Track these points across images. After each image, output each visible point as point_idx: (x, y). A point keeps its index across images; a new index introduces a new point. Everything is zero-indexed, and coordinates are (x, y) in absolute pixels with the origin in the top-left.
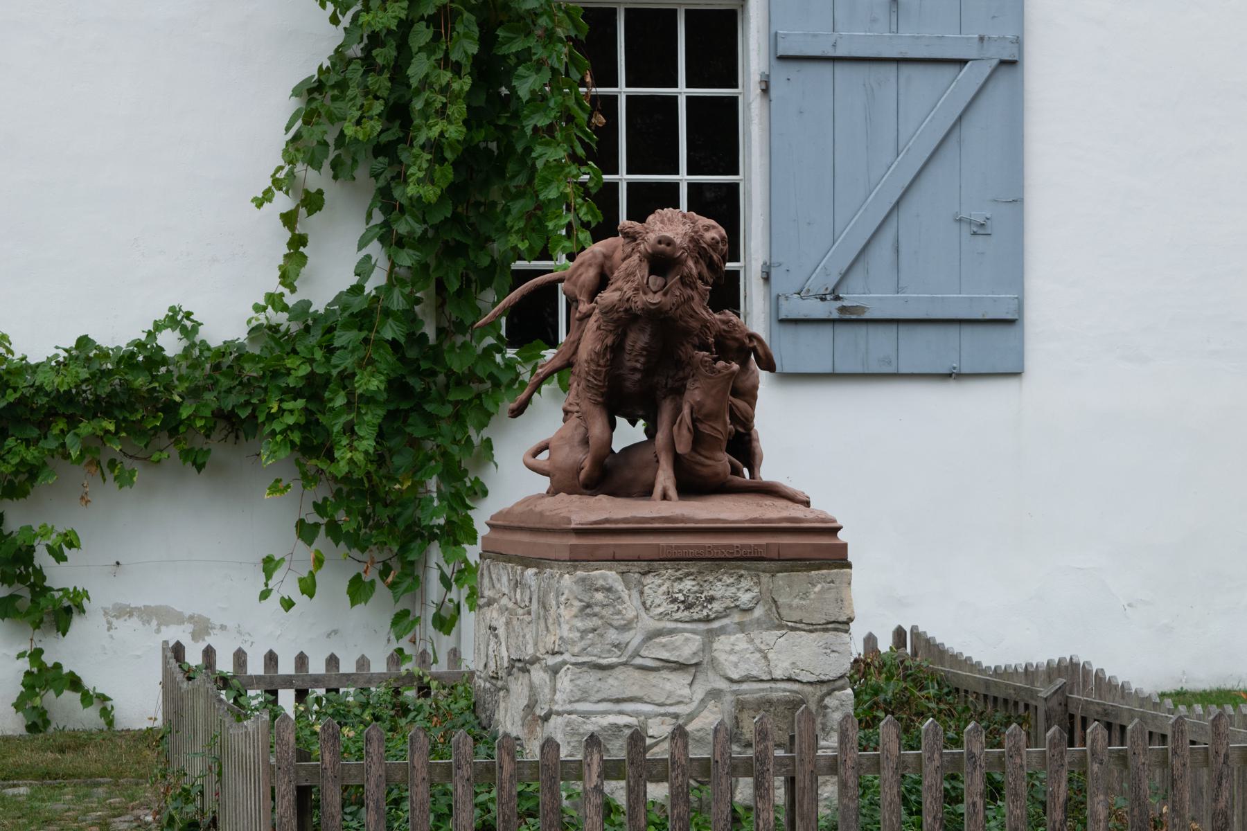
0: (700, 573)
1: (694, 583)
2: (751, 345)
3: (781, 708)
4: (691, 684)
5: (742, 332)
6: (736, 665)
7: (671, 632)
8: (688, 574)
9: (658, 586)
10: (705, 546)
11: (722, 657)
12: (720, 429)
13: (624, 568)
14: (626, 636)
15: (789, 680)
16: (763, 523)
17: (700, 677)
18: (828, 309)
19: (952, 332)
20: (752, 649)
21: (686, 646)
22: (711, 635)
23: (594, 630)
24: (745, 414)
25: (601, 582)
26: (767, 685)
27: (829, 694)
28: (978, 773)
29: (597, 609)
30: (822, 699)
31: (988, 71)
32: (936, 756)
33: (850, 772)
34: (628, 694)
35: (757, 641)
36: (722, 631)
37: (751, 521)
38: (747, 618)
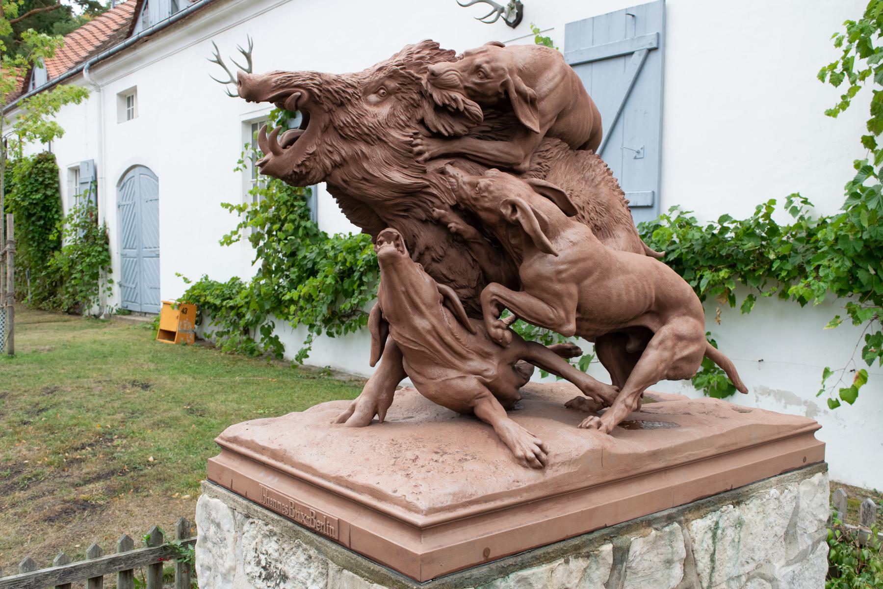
1: (276, 546)
2: (514, 218)
5: (495, 199)
8: (272, 534)
12: (408, 336)
13: (233, 505)
16: (347, 487)
24: (534, 315)
37: (338, 480)
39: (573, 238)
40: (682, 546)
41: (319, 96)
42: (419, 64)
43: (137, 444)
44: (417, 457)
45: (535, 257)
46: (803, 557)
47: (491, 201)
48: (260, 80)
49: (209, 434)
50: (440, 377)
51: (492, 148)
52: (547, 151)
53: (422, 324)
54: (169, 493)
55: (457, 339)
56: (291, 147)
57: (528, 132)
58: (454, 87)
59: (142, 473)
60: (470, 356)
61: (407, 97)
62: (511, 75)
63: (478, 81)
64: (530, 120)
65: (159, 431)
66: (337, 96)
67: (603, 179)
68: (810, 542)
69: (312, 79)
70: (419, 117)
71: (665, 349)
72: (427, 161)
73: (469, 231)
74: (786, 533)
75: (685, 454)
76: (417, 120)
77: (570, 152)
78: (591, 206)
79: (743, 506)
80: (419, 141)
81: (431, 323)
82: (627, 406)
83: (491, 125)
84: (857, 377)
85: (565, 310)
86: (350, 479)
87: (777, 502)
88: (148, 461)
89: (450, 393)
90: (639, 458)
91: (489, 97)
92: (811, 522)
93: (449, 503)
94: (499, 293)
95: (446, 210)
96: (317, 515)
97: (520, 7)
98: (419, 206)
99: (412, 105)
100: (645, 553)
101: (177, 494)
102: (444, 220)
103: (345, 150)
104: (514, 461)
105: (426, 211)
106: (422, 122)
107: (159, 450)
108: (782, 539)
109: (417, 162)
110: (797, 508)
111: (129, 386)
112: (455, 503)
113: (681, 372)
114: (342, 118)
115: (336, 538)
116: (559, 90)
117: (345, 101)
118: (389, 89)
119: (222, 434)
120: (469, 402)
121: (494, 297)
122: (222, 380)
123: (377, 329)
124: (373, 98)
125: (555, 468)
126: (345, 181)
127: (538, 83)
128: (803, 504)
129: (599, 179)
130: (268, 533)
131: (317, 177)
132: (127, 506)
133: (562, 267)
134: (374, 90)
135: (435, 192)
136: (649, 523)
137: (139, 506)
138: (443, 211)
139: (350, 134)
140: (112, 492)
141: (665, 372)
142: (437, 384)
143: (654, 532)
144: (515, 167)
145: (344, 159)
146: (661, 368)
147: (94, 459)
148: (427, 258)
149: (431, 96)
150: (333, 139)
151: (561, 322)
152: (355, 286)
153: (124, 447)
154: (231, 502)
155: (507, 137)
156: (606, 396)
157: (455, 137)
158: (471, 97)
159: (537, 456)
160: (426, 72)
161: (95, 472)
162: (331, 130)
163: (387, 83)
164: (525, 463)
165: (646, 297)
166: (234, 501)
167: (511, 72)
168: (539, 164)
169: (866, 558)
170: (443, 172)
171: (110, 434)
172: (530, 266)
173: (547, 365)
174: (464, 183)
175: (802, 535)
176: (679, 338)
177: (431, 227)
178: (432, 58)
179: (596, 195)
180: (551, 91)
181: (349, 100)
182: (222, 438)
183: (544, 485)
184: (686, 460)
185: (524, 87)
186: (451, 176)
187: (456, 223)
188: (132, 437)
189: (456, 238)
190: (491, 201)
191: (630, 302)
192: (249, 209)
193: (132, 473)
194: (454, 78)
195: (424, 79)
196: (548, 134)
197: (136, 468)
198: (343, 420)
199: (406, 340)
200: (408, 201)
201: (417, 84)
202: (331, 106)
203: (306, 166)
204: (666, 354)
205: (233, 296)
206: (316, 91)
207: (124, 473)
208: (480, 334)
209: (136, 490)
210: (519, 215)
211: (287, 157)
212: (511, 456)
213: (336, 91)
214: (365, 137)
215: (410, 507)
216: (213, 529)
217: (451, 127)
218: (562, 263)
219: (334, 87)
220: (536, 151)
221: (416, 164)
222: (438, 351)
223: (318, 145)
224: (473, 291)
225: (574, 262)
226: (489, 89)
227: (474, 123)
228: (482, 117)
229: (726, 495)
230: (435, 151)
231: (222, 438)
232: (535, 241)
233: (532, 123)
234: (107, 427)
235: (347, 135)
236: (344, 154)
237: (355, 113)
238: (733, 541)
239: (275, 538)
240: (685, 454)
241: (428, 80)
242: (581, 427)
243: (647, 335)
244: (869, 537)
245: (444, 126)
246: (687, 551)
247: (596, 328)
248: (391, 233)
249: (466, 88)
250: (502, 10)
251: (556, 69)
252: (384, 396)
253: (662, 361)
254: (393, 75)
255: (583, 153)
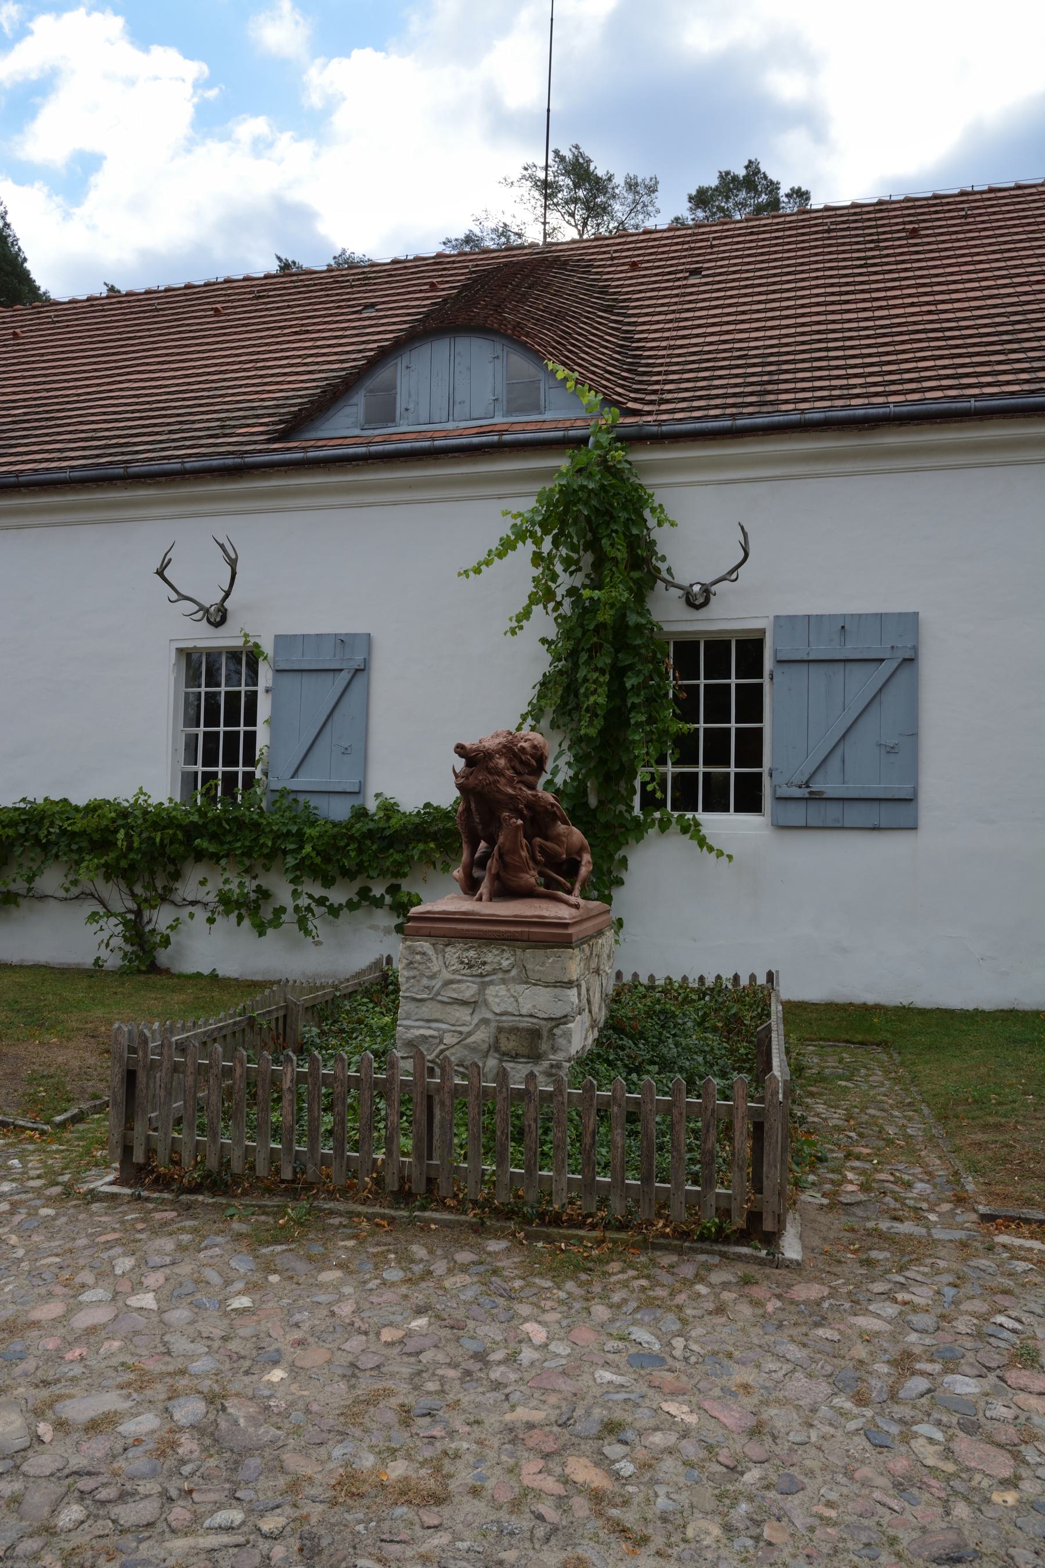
0: (479, 947)
3: (524, 1034)
4: (472, 1014)
6: (498, 1005)
7: (459, 982)
9: (453, 953)
11: (490, 999)
14: (433, 983)
15: (531, 1016)
17: (477, 1010)
18: (803, 792)
19: (876, 804)
20: (508, 995)
21: (468, 990)
22: (484, 986)
23: (414, 977)
25: (419, 949)
26: (517, 1018)
27: (557, 1026)
28: (532, 1104)
29: (416, 965)
30: (552, 1029)
31: (896, 665)
32: (504, 1090)
33: (446, 1095)
34: (433, 1017)
35: (512, 991)
36: (491, 983)
38: (507, 976)
254: (505, 746)
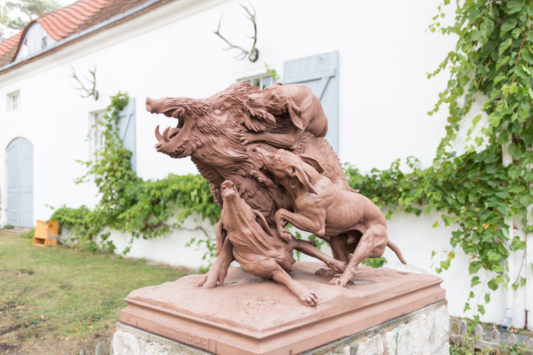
2: (294, 175)
5: (284, 165)
8: (165, 349)
10: (176, 330)
12: (239, 238)
16: (213, 321)
24: (304, 225)
37: (207, 317)
39: (323, 185)
40: (382, 346)
41: (190, 111)
42: (242, 94)
43: (32, 308)
44: (249, 303)
45: (304, 195)
46: (438, 350)
47: (281, 166)
48: (159, 102)
49: (76, 300)
50: (255, 260)
51: (279, 138)
52: (304, 139)
53: (247, 231)
54: (58, 337)
55: (264, 239)
56: (174, 138)
57: (297, 129)
58: (261, 107)
59: (38, 325)
60: (271, 248)
61: (235, 111)
62: (289, 100)
63: (273, 103)
64: (298, 123)
65: (45, 300)
66: (200, 111)
67: (330, 152)
68: (441, 343)
69: (187, 102)
70: (242, 122)
71: (369, 242)
72: (246, 144)
73: (269, 181)
74: (430, 338)
75: (381, 297)
76: (240, 123)
77: (314, 139)
78: (325, 167)
79: (409, 324)
80: (242, 134)
81: (251, 231)
82: (351, 272)
83: (278, 126)
84: (449, 255)
85: (320, 222)
86: (214, 316)
87: (425, 321)
88: (41, 318)
89: (261, 268)
90: (359, 299)
91: (278, 111)
92: (441, 331)
93: (272, 326)
94: (285, 214)
95: (257, 171)
96: (195, 337)
97: (257, 52)
98: (242, 169)
99: (238, 116)
100: (365, 351)
101: (63, 337)
102: (256, 176)
103: (203, 139)
104: (300, 303)
105: (246, 171)
106: (243, 124)
107: (46, 311)
108: (428, 341)
109: (241, 145)
110: (434, 324)
111: (20, 273)
112: (275, 326)
113: (376, 254)
114: (202, 122)
115: (207, 349)
116: (312, 108)
117: (204, 113)
118: (226, 107)
119: (128, 296)
120: (270, 273)
121: (283, 216)
122: (79, 267)
123: (221, 235)
124: (218, 111)
125: (321, 306)
126: (203, 156)
127: (301, 104)
128: (437, 322)
129: (328, 152)
130: (163, 350)
131: (188, 153)
132: (32, 345)
133: (318, 200)
134: (218, 107)
135: (251, 161)
136: (366, 334)
137: (40, 345)
138: (255, 171)
139: (206, 130)
140: (21, 338)
141: (370, 254)
142: (254, 263)
143: (369, 339)
144: (290, 148)
145: (203, 144)
146: (368, 252)
147: (6, 318)
148: (246, 196)
149: (249, 111)
150: (196, 133)
151: (318, 229)
152: (162, 209)
153: (24, 310)
154: (137, 334)
155: (286, 131)
156: (340, 267)
157: (261, 132)
158: (269, 111)
159: (312, 300)
160: (245, 99)
161: (8, 326)
162: (196, 128)
163: (225, 104)
164: (306, 303)
165: (359, 215)
166: (139, 333)
167: (289, 99)
168: (301, 145)
169: (464, 352)
170: (254, 150)
171: (13, 303)
172: (302, 199)
173: (309, 252)
174: (266, 157)
175: (437, 339)
176: (376, 236)
177: (248, 179)
178: (248, 91)
179: (327, 161)
180: (308, 108)
181: (206, 113)
182: (129, 298)
183: (316, 315)
184: (382, 300)
185: (296, 107)
186: (259, 153)
187: (262, 177)
188: (28, 304)
189: (262, 186)
190: (281, 166)
191: (351, 217)
192: (94, 163)
193: (32, 326)
194: (261, 102)
195: (245, 102)
196: (305, 131)
197: (33, 323)
198: (201, 285)
199: (237, 240)
200: (237, 166)
201: (241, 104)
202: (196, 116)
203: (183, 148)
204: (370, 244)
205: (82, 217)
206: (189, 108)
207: (26, 326)
208: (274, 236)
209: (37, 336)
210: (296, 173)
211: (172, 142)
212: (298, 300)
213: (199, 108)
214: (214, 132)
215: (251, 329)
216: (125, 350)
217: (259, 127)
218: (319, 198)
219: (198, 106)
220: (300, 139)
221: (241, 146)
222: (254, 246)
223: (189, 137)
224: (269, 213)
225: (324, 197)
226: (279, 107)
227: (271, 125)
228: (275, 122)
229: (401, 318)
230: (250, 139)
231: (129, 298)
232: (305, 187)
233: (299, 124)
234: (10, 299)
235: (205, 131)
236: (203, 141)
237: (209, 120)
238: (405, 343)
239: (167, 352)
240: (381, 297)
241: (247, 103)
242: (330, 284)
243: (358, 235)
244: (464, 341)
245: (255, 127)
246: (384, 349)
247: (334, 231)
248: (229, 183)
249: (267, 107)
250: (247, 53)
251: (310, 97)
252: (223, 271)
253: (368, 248)
255: (319, 139)
